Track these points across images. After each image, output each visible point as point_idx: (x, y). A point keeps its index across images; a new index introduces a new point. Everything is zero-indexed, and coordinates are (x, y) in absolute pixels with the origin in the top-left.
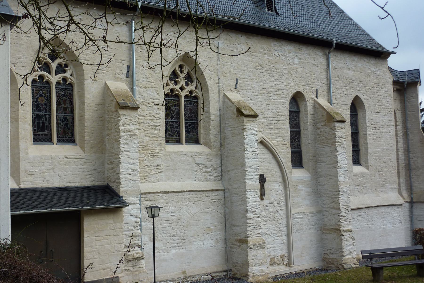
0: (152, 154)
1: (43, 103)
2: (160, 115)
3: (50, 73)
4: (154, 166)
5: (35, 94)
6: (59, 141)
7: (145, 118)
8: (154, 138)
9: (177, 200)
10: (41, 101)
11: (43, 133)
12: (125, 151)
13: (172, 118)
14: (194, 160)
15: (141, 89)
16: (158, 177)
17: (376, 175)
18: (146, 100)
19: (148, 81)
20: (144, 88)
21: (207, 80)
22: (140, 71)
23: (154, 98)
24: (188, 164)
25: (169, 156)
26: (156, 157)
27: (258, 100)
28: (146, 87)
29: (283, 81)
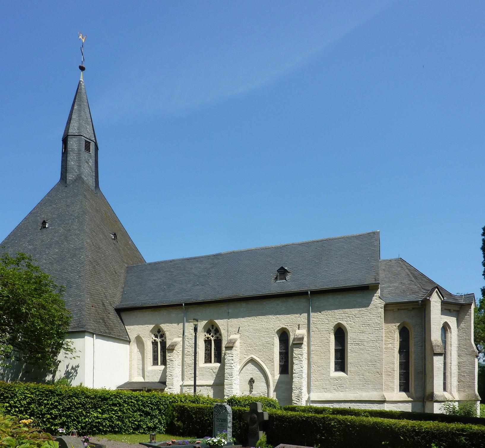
6: (161, 364)
11: (156, 361)
17: (356, 378)
27: (252, 337)
28: (191, 339)
29: (272, 323)
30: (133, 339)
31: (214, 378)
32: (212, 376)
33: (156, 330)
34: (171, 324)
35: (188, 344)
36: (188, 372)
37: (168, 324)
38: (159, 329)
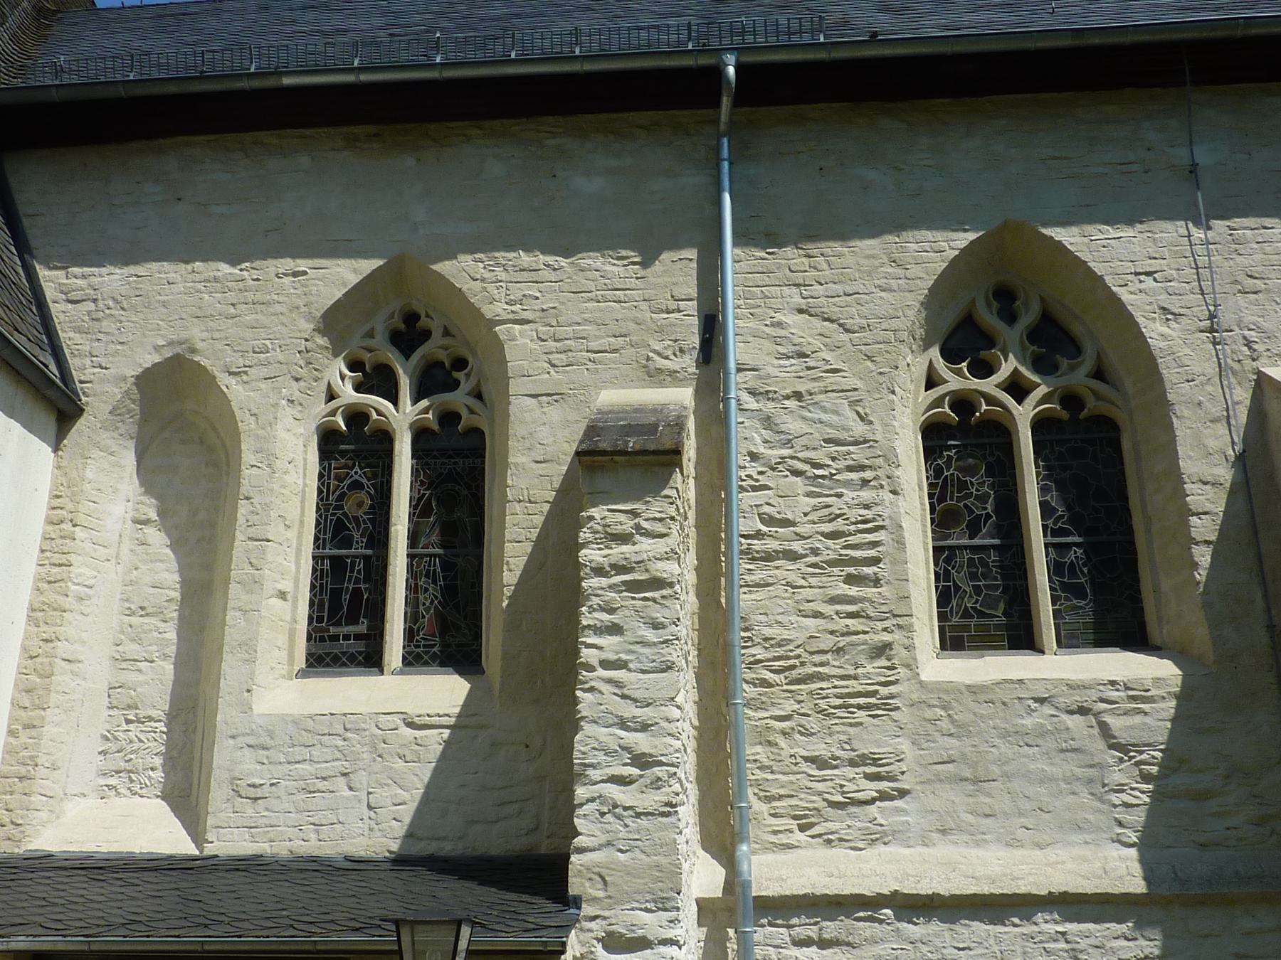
0: (840, 702)
1: (360, 513)
2: (879, 508)
3: (394, 400)
4: (852, 763)
5: (333, 482)
7: (797, 530)
8: (849, 622)
9: (996, 949)
10: (357, 505)
12: (605, 664)
13: (974, 530)
14: (1104, 728)
15: (770, 405)
16: (883, 822)
18: (798, 448)
19: (809, 368)
20: (787, 397)
21: (1141, 320)
22: (766, 329)
23: (843, 435)
24: (1062, 751)
25: (944, 708)
26: (861, 713)
28: (798, 396)
30: (116, 392)
31: (1138, 817)
32: (1101, 788)
33: (380, 325)
34: (563, 262)
35: (761, 449)
36: (782, 742)
37: (525, 259)
38: (411, 318)
